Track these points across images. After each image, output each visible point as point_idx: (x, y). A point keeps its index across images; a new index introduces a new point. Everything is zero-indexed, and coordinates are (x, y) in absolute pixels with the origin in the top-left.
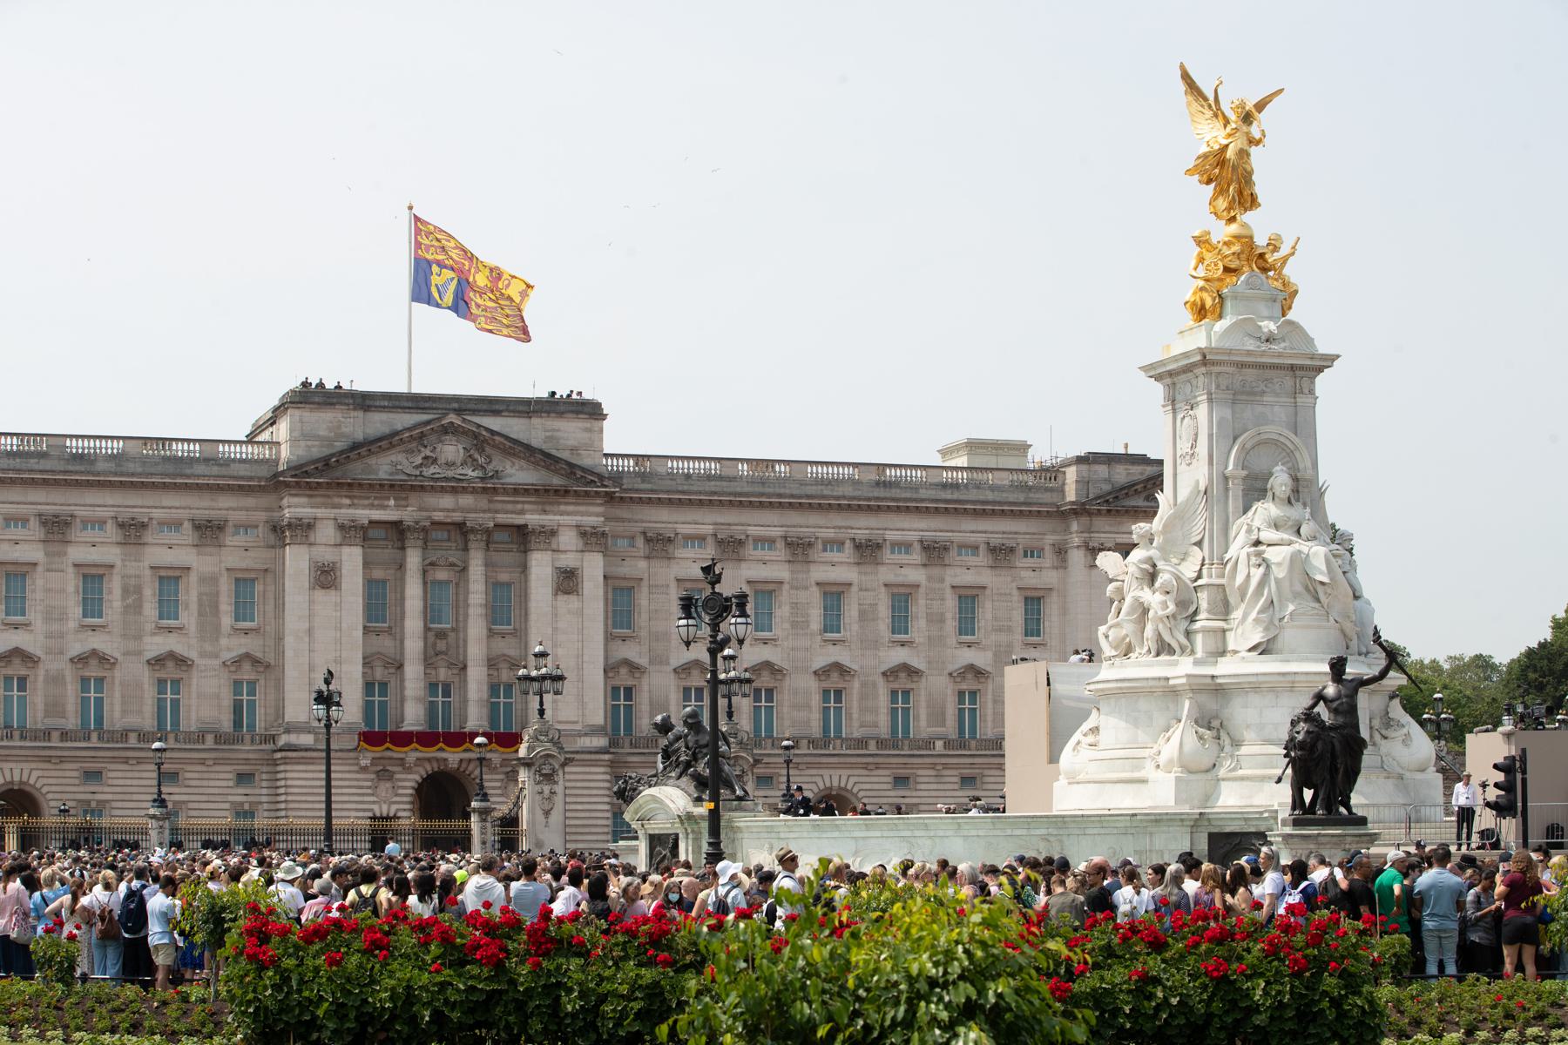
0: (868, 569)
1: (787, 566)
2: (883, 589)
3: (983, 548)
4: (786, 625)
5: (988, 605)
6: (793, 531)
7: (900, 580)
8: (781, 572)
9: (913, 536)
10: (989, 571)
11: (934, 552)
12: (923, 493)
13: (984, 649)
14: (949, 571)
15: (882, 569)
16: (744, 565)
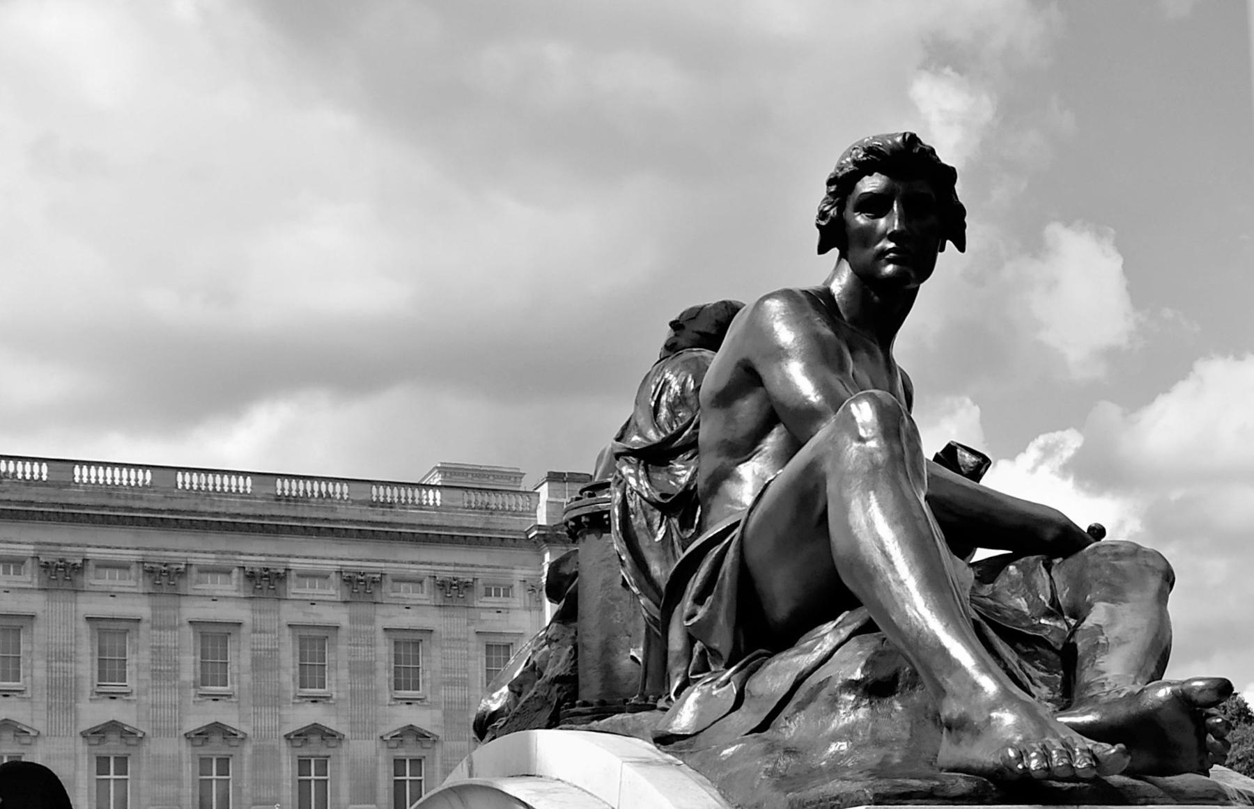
0: (265, 605)
1: (146, 599)
2: (287, 631)
3: (427, 581)
4: (146, 676)
5: (436, 652)
6: (155, 556)
7: (311, 620)
8: (141, 608)
9: (330, 566)
10: (436, 611)
11: (360, 587)
12: (342, 513)
13: (431, 706)
14: (381, 610)
15: (285, 606)
16: (81, 598)
